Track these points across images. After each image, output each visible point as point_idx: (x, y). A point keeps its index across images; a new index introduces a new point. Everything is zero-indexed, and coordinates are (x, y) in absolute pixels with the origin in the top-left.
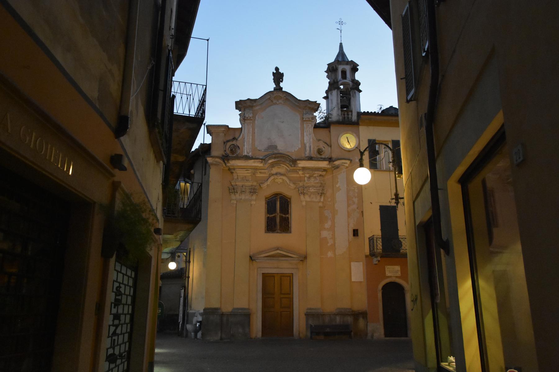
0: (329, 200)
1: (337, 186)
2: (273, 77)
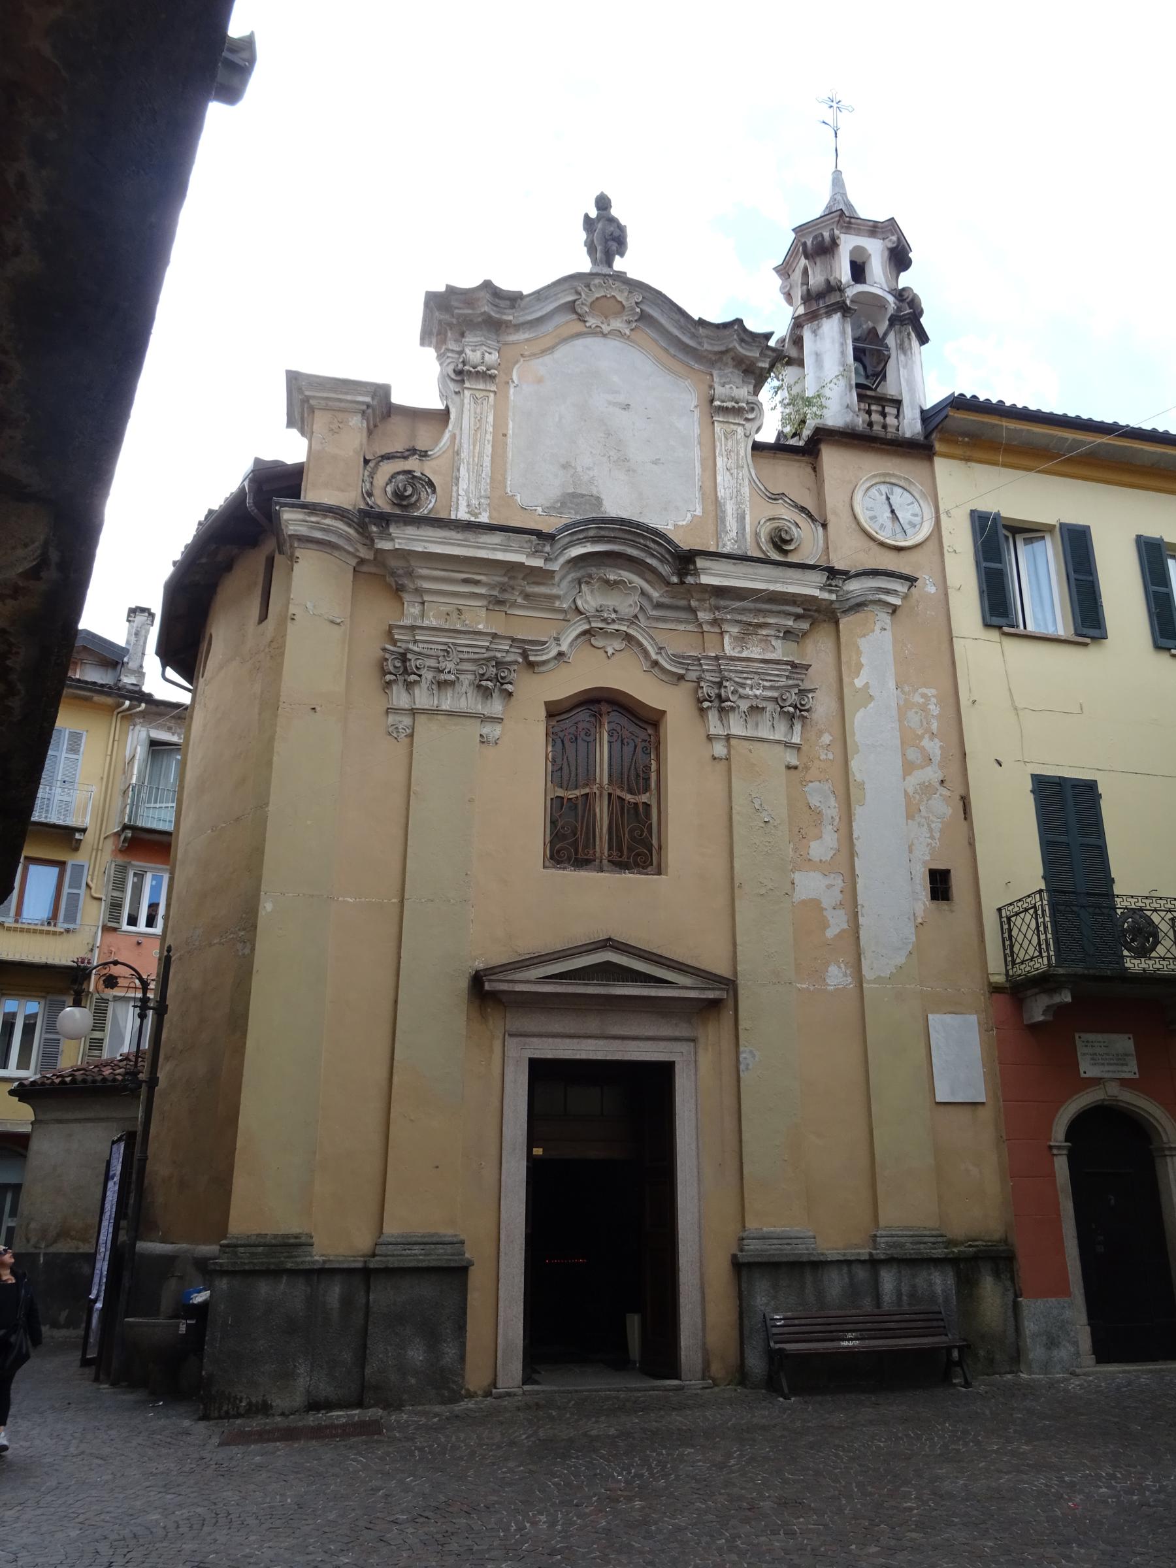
0: (826, 739)
1: (859, 683)
2: (583, 236)
